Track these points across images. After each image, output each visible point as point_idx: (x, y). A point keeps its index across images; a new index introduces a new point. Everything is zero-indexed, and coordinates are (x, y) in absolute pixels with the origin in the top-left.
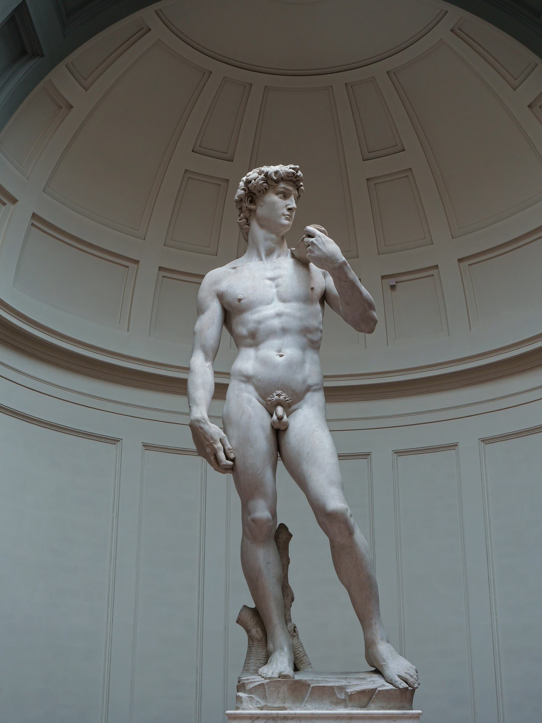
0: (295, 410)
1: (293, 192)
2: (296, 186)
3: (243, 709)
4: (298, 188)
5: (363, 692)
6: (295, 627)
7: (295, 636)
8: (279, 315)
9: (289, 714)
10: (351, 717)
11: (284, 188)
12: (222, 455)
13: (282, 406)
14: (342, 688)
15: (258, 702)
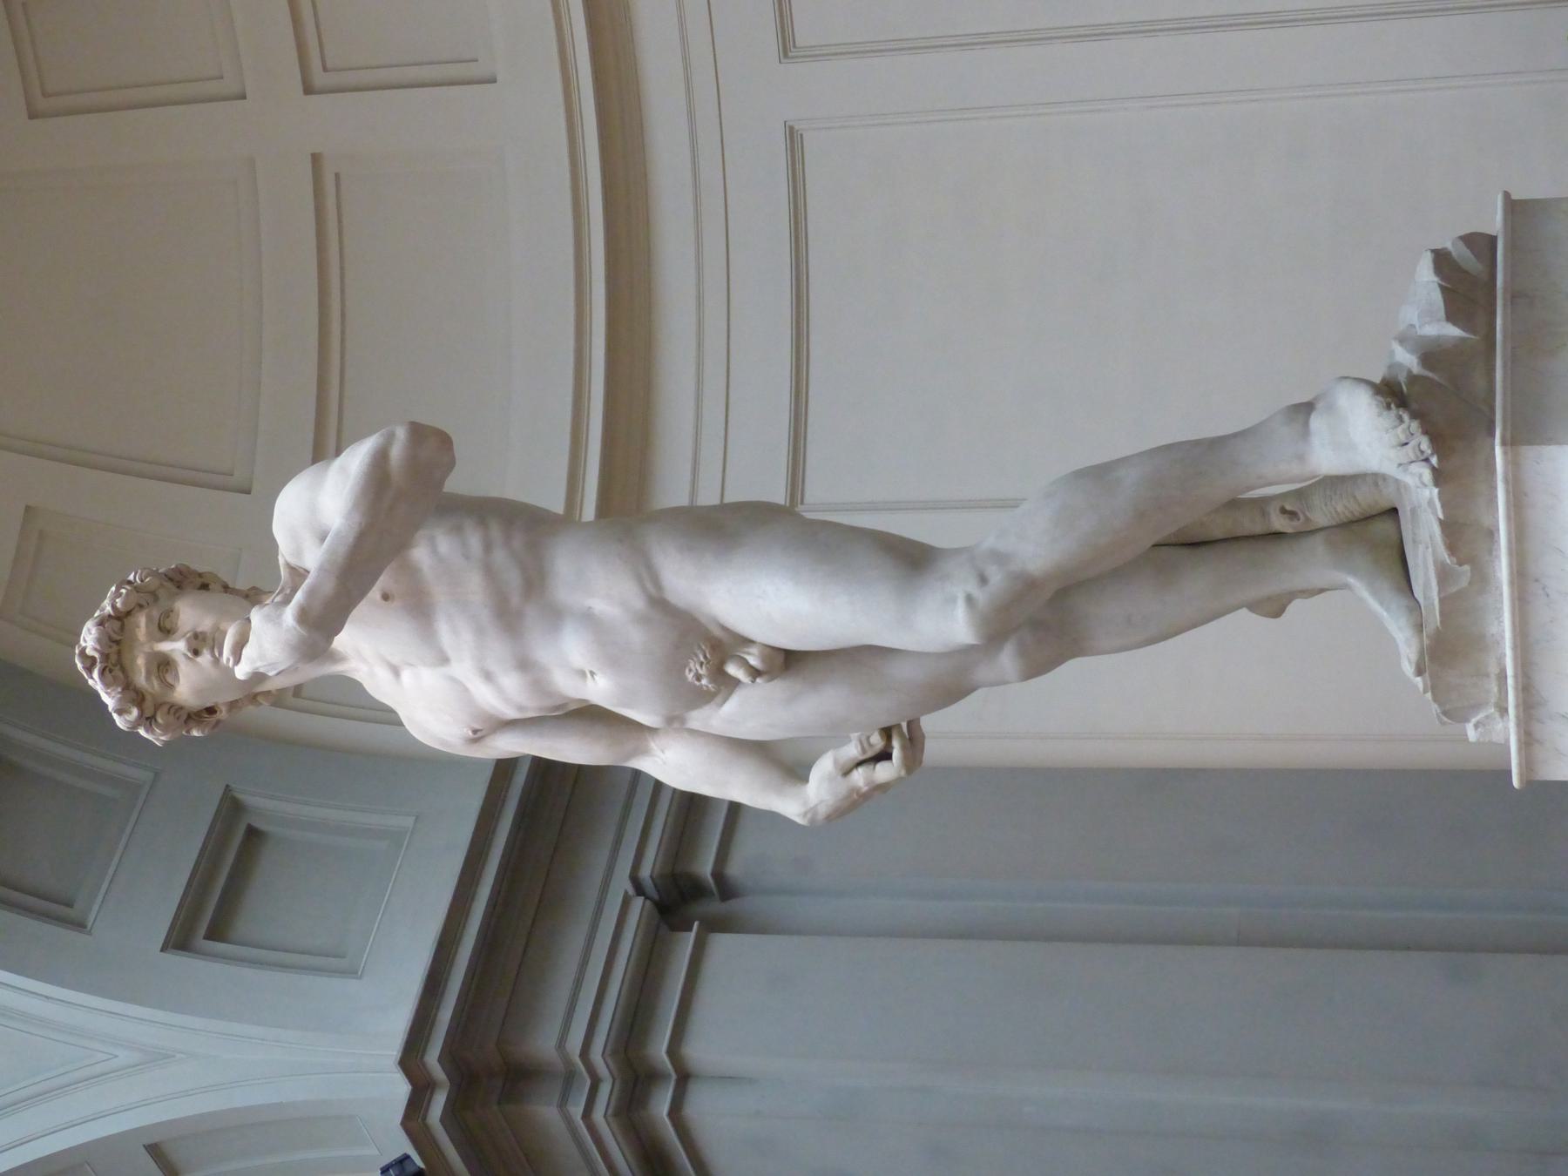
0: (725, 629)
1: (147, 649)
2: (122, 628)
3: (1508, 740)
4: (121, 618)
5: (1452, 548)
6: (1283, 511)
7: (1307, 519)
8: (488, 676)
9: (1516, 689)
10: (1521, 575)
11: (148, 678)
12: (883, 772)
13: (722, 663)
14: (1444, 575)
15: (1487, 717)
